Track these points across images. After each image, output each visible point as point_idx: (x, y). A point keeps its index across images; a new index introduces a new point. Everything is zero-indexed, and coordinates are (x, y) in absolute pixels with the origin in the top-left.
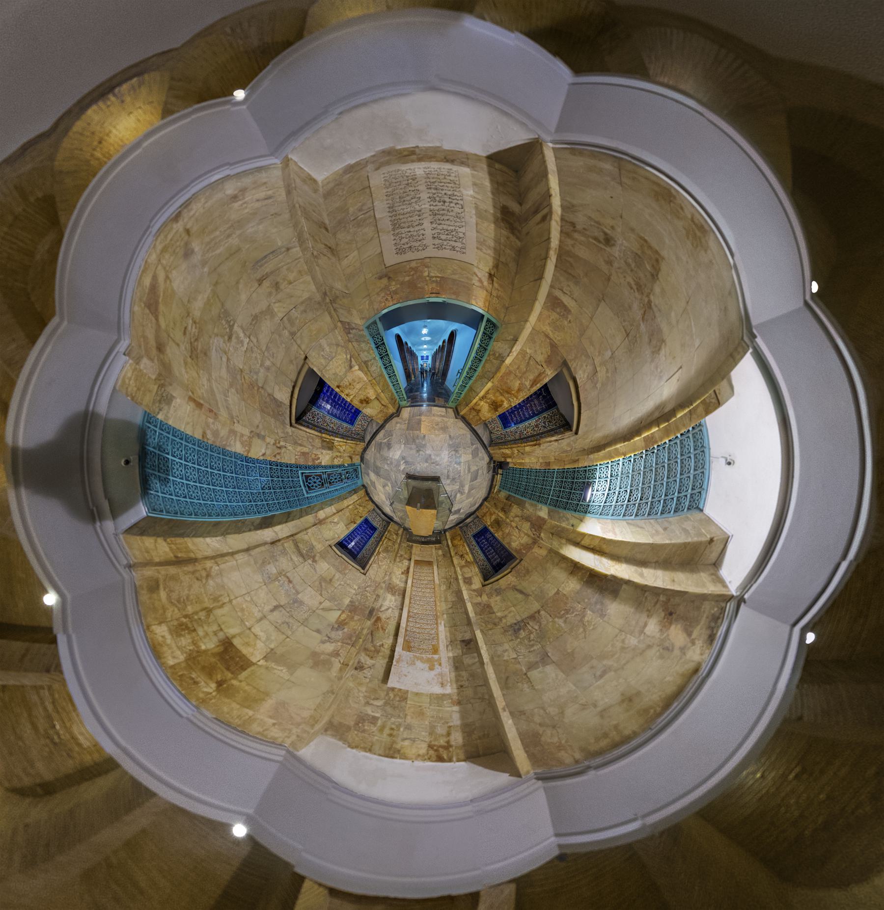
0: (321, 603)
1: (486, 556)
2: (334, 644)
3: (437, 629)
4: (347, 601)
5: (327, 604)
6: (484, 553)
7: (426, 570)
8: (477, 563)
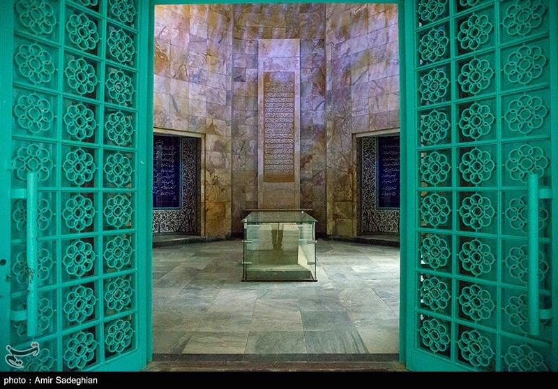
0: (370, 75)
1: (177, 164)
3: (265, 98)
4: (353, 95)
5: (365, 79)
6: (177, 171)
7: (276, 169)
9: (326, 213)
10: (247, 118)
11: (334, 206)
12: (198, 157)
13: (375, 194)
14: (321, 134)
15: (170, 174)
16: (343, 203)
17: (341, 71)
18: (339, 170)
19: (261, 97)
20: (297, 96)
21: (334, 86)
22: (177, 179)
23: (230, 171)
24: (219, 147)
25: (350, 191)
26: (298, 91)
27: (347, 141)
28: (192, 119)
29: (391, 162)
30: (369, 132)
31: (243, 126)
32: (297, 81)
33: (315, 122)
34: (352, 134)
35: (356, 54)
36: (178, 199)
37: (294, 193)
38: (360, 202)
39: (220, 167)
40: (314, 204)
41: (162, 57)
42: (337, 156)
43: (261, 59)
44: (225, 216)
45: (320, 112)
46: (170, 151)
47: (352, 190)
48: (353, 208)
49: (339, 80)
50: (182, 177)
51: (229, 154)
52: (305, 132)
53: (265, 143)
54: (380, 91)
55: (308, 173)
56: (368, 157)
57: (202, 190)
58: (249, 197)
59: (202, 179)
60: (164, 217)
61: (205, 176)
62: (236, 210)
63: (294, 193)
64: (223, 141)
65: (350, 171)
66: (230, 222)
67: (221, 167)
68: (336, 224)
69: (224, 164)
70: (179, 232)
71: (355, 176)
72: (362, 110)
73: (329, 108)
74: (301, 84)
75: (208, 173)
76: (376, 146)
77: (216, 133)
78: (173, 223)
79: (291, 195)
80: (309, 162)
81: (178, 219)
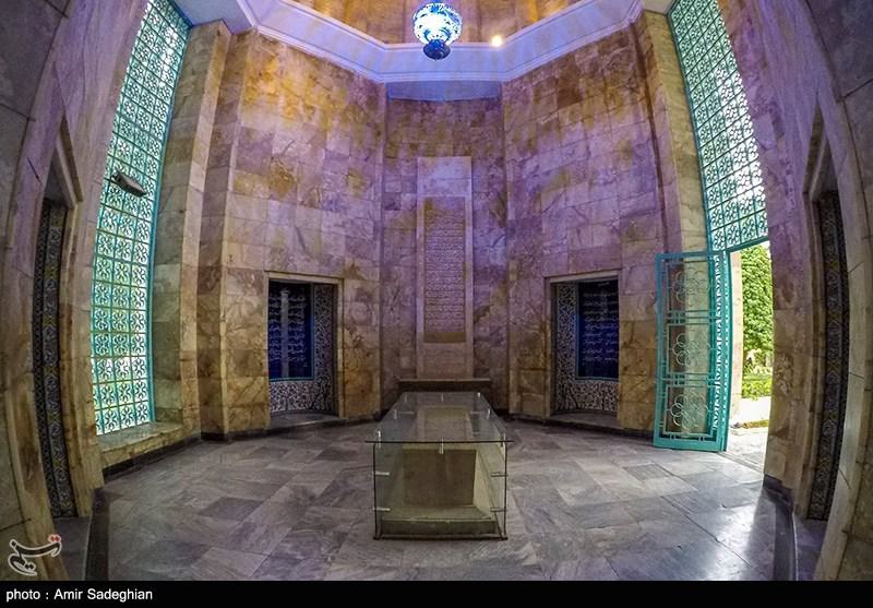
0: (567, 199)
2: (528, 173)
5: (561, 204)
8: (333, 320)
9: (508, 385)
10: (402, 256)
11: (519, 375)
12: (334, 310)
13: (573, 360)
14: (501, 276)
15: (298, 332)
16: (532, 372)
17: (527, 194)
18: (527, 327)
19: (420, 229)
20: (469, 229)
21: (518, 214)
22: (308, 340)
23: (377, 329)
24: (363, 296)
25: (542, 356)
26: (469, 221)
27: (538, 287)
28: (326, 260)
29: (594, 316)
30: (568, 275)
31: (396, 268)
32: (469, 209)
33: (492, 261)
34: (546, 278)
35: (548, 173)
36: (309, 365)
37: (465, 355)
38: (555, 372)
39: (362, 324)
40: (492, 372)
41: (286, 178)
42: (526, 306)
43: (420, 183)
44: (371, 390)
45: (500, 249)
46: (299, 303)
47: (545, 354)
48: (546, 377)
49: (525, 206)
50: (315, 336)
51: (377, 306)
52: (480, 274)
53: (426, 291)
54: (581, 219)
55: (484, 331)
56: (565, 309)
57: (340, 356)
58: (405, 362)
59: (340, 340)
60: (292, 390)
61: (343, 336)
62: (388, 379)
63: (465, 355)
64: (368, 289)
65: (542, 329)
66: (378, 397)
67: (366, 323)
68: (522, 401)
69: (370, 320)
70: (312, 410)
71: (549, 335)
72: (558, 245)
73: (512, 243)
74: (474, 213)
75: (347, 332)
76: (574, 295)
77: (359, 278)
78: (304, 397)
79: (461, 360)
80: (484, 315)
81: (310, 392)
